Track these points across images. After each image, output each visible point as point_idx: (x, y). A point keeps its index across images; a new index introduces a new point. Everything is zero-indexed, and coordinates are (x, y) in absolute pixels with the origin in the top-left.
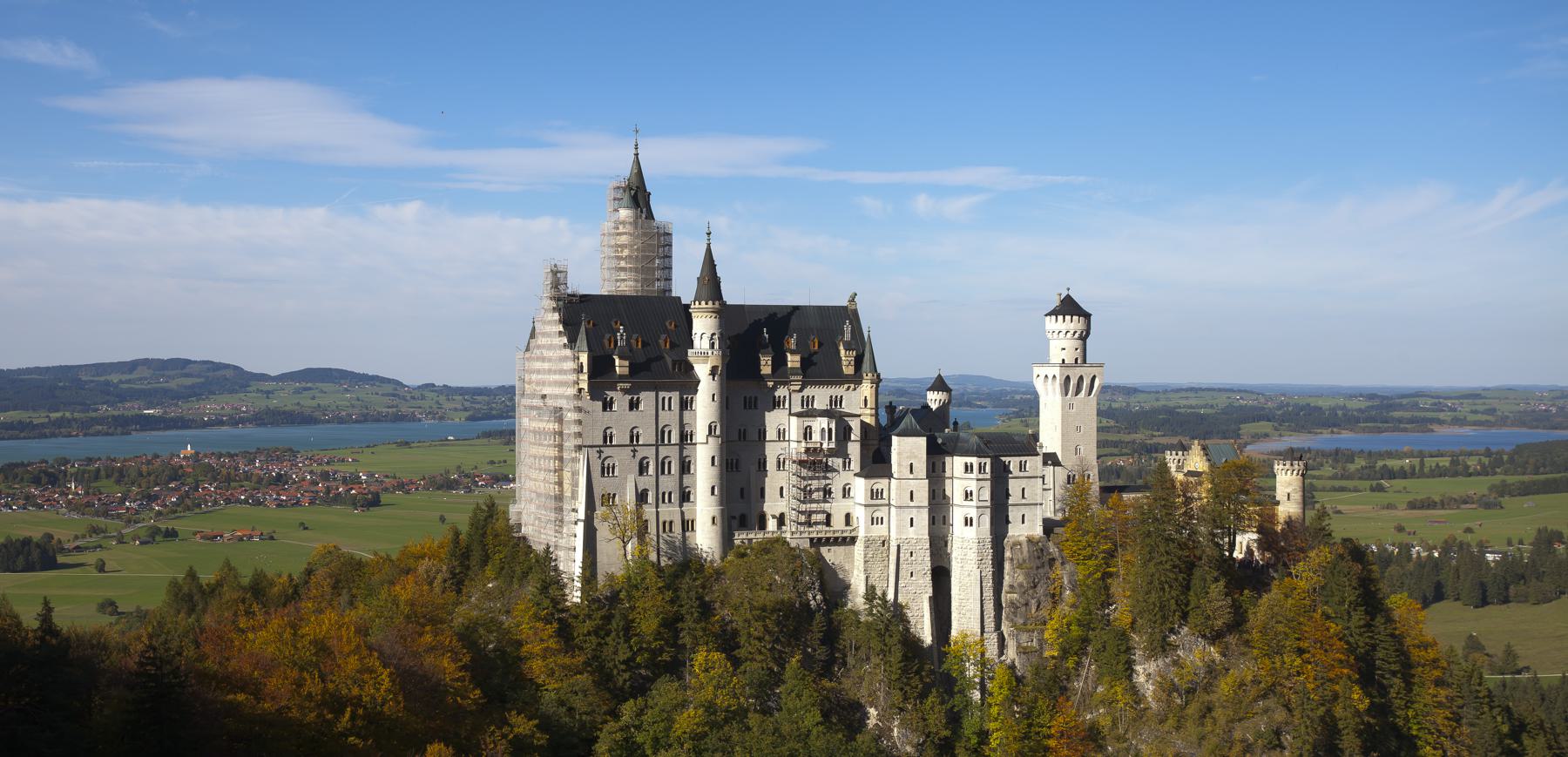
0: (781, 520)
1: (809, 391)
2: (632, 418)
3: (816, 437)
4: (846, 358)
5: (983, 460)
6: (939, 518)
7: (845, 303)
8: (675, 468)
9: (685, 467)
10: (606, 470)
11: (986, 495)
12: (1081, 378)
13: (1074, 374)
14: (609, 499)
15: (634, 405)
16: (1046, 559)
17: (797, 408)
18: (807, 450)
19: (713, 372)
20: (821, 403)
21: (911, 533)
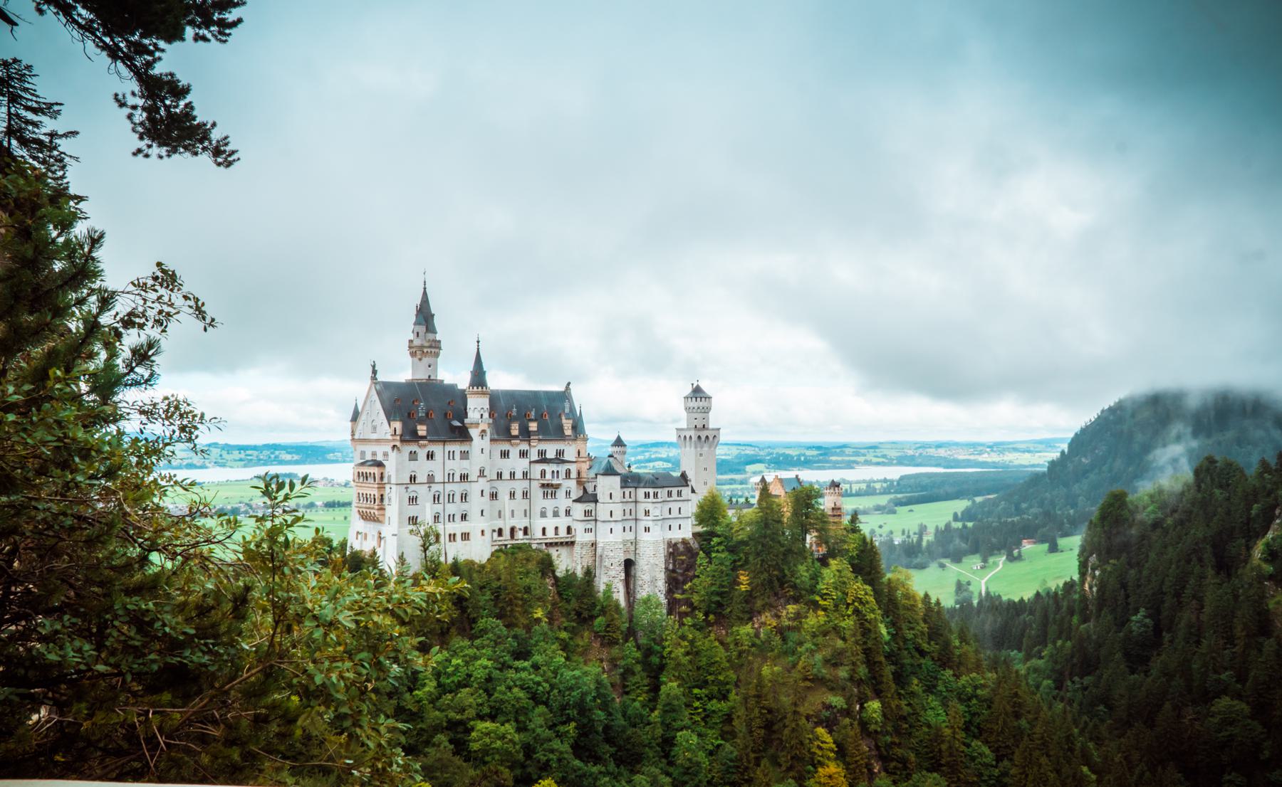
0: (526, 531)
1: (542, 446)
3: (548, 476)
4: (567, 425)
6: (627, 529)
7: (562, 389)
8: (457, 498)
9: (464, 497)
10: (413, 500)
11: (657, 512)
13: (703, 434)
14: (413, 520)
15: (430, 456)
17: (535, 457)
20: (551, 454)
21: (611, 538)
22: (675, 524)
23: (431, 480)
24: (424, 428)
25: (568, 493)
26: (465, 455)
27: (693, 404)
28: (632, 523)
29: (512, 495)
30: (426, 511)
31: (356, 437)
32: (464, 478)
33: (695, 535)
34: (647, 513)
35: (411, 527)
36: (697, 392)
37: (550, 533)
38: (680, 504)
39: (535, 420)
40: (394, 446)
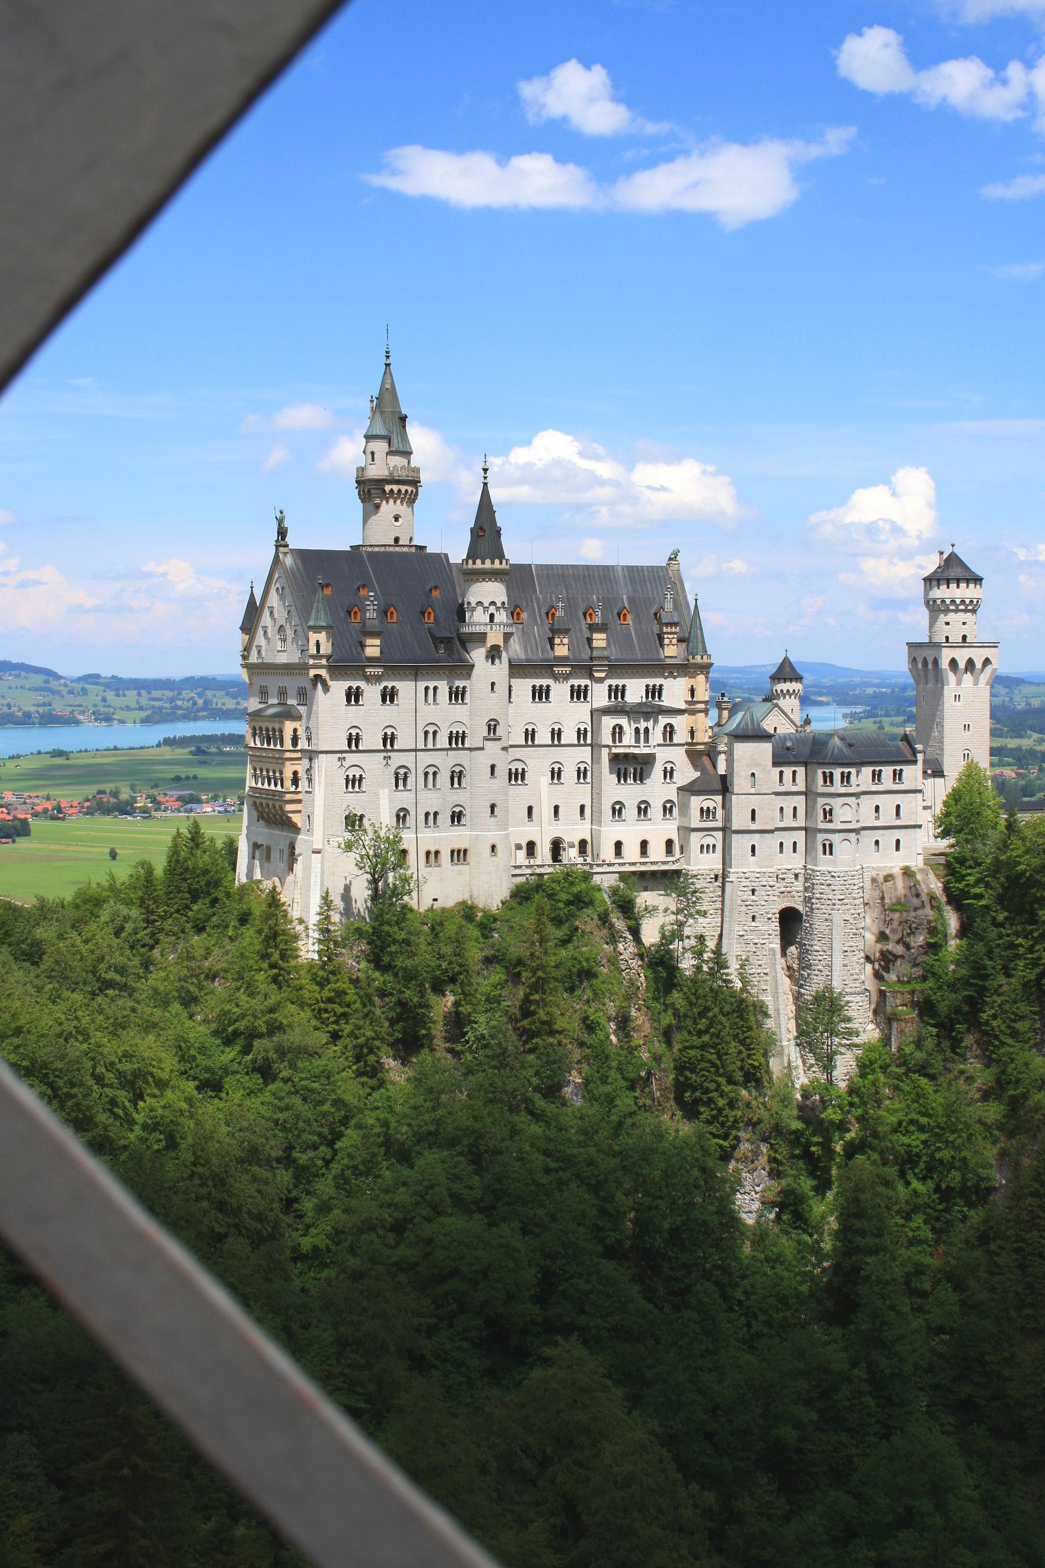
2: (387, 714)
3: (628, 738)
5: (846, 770)
6: (788, 846)
8: (444, 778)
9: (457, 777)
12: (970, 663)
13: (962, 656)
15: (389, 696)
16: (924, 898)
18: (615, 758)
19: (494, 654)
22: (888, 839)
23: (389, 739)
24: (377, 642)
25: (668, 774)
26: (457, 695)
27: (942, 593)
28: (800, 837)
29: (556, 775)
30: (380, 806)
31: (253, 659)
32: (457, 739)
33: (932, 859)
34: (828, 814)
35: (348, 836)
36: (952, 570)
37: (631, 852)
38: (898, 799)
39: (602, 628)
40: (317, 676)
